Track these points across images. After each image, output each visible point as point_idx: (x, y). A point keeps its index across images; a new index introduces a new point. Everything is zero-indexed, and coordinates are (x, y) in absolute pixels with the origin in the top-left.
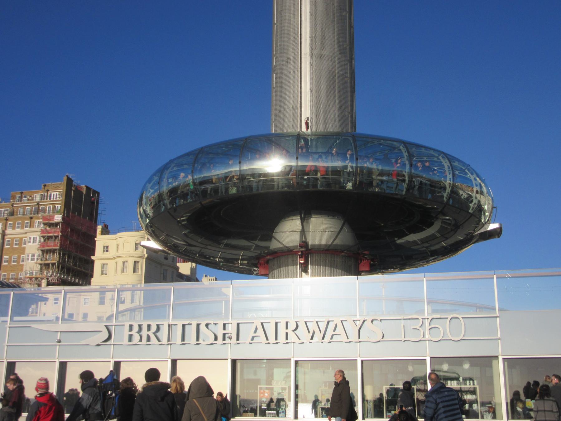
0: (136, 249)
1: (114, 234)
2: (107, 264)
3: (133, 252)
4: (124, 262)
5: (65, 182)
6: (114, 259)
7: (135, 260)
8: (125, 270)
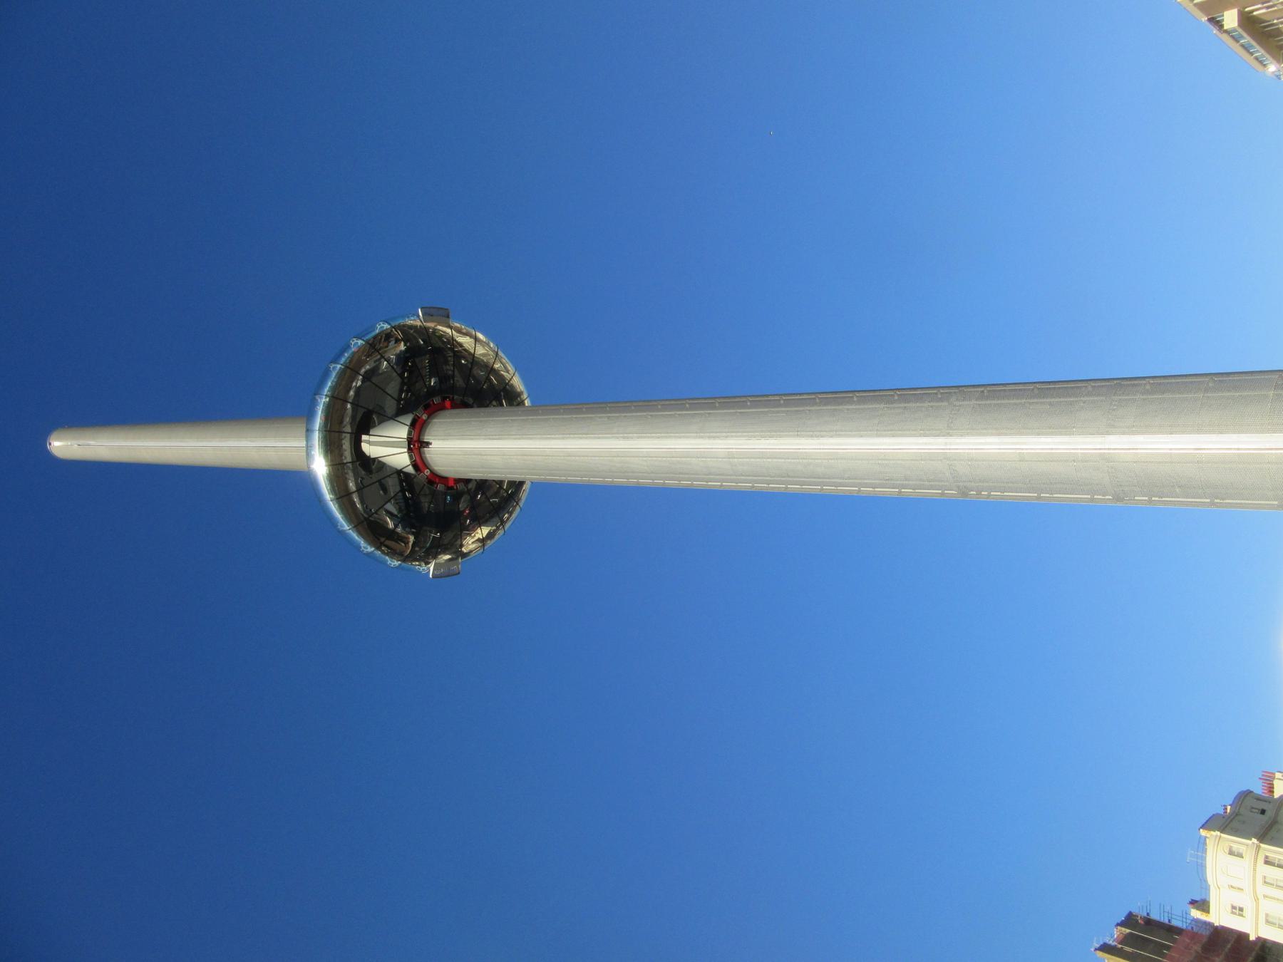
0: (1240, 855)
1: (1209, 890)
2: (1267, 915)
4: (1265, 882)
5: (1106, 955)
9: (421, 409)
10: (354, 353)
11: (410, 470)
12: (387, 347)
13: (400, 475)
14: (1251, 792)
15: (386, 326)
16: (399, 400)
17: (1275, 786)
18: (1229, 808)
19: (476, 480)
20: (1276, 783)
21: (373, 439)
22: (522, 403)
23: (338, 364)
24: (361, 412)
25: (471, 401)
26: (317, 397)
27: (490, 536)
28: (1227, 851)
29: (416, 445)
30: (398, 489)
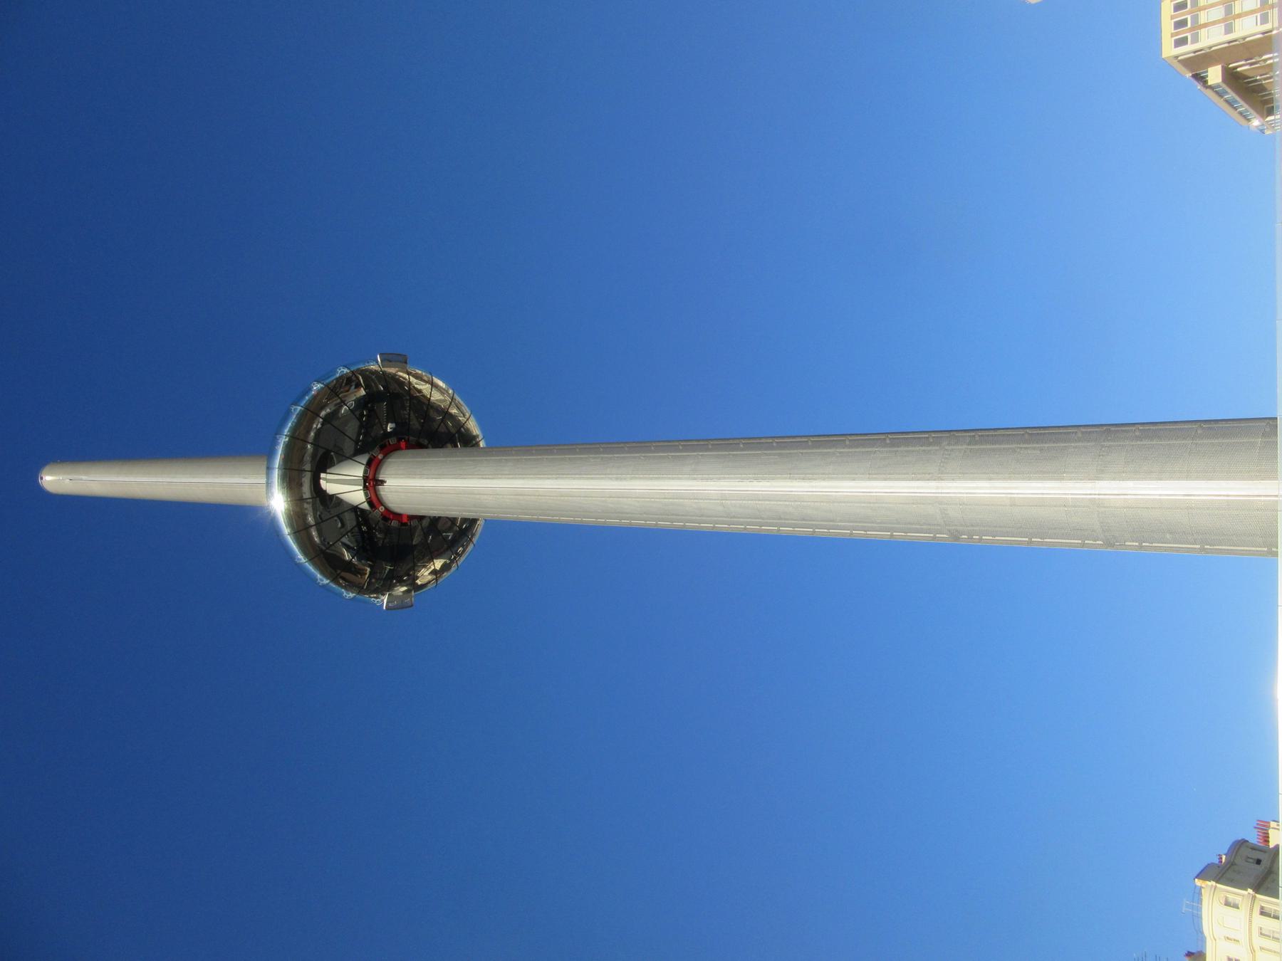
0: (1236, 906)
1: (1205, 942)
3: (1242, 913)
6: (1254, 951)
7: (1259, 912)
8: (1276, 936)
9: (377, 449)
10: (315, 397)
11: (366, 506)
12: (348, 391)
13: (356, 512)
14: (1248, 841)
15: (346, 371)
16: (357, 442)
17: (1270, 836)
18: (1224, 857)
19: (430, 517)
20: (1271, 832)
21: (329, 477)
22: (477, 444)
23: (299, 406)
24: (321, 452)
25: (426, 442)
26: (278, 436)
27: (445, 568)
28: (1223, 902)
29: (371, 483)
30: (354, 523)
